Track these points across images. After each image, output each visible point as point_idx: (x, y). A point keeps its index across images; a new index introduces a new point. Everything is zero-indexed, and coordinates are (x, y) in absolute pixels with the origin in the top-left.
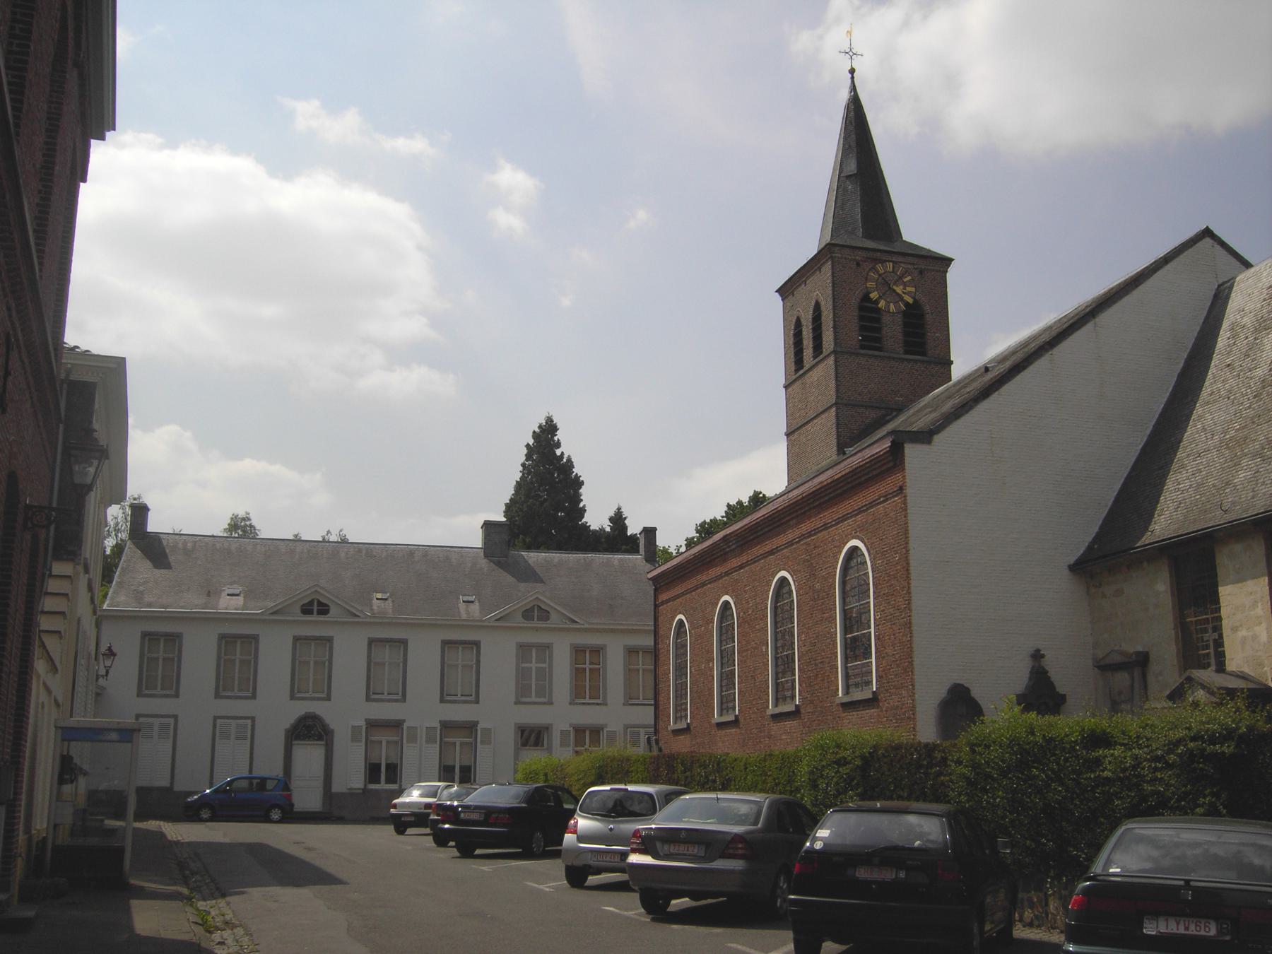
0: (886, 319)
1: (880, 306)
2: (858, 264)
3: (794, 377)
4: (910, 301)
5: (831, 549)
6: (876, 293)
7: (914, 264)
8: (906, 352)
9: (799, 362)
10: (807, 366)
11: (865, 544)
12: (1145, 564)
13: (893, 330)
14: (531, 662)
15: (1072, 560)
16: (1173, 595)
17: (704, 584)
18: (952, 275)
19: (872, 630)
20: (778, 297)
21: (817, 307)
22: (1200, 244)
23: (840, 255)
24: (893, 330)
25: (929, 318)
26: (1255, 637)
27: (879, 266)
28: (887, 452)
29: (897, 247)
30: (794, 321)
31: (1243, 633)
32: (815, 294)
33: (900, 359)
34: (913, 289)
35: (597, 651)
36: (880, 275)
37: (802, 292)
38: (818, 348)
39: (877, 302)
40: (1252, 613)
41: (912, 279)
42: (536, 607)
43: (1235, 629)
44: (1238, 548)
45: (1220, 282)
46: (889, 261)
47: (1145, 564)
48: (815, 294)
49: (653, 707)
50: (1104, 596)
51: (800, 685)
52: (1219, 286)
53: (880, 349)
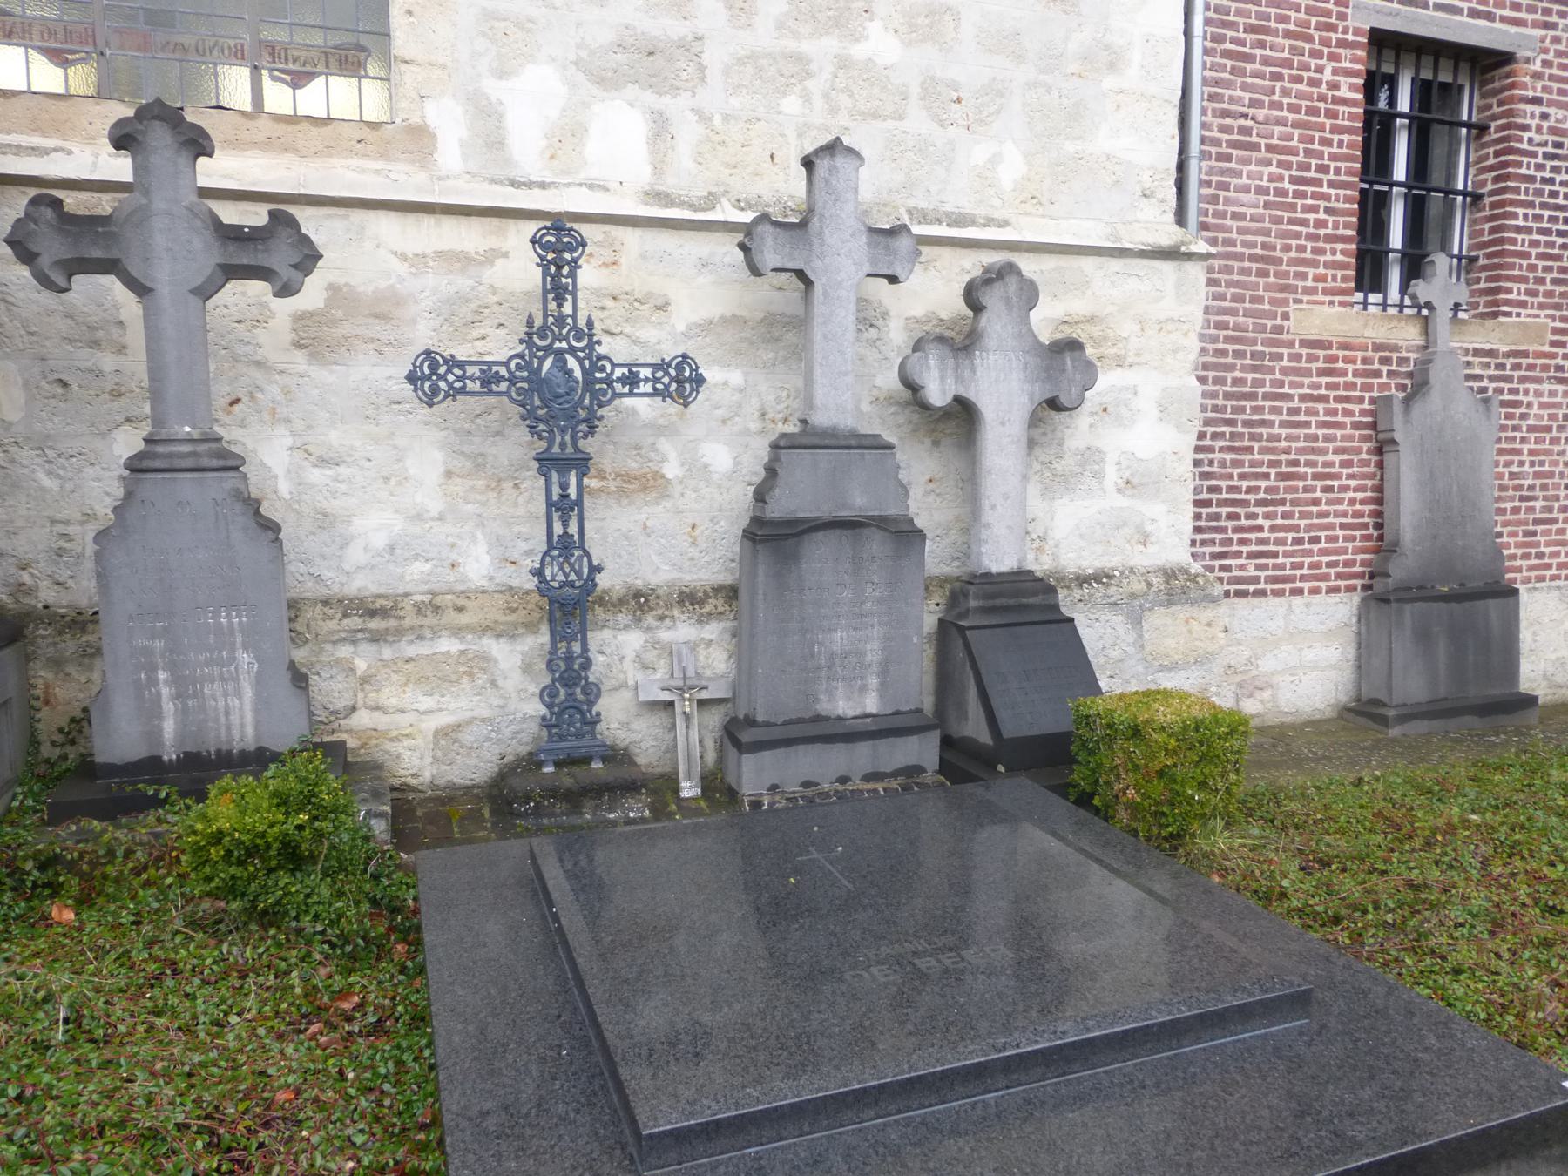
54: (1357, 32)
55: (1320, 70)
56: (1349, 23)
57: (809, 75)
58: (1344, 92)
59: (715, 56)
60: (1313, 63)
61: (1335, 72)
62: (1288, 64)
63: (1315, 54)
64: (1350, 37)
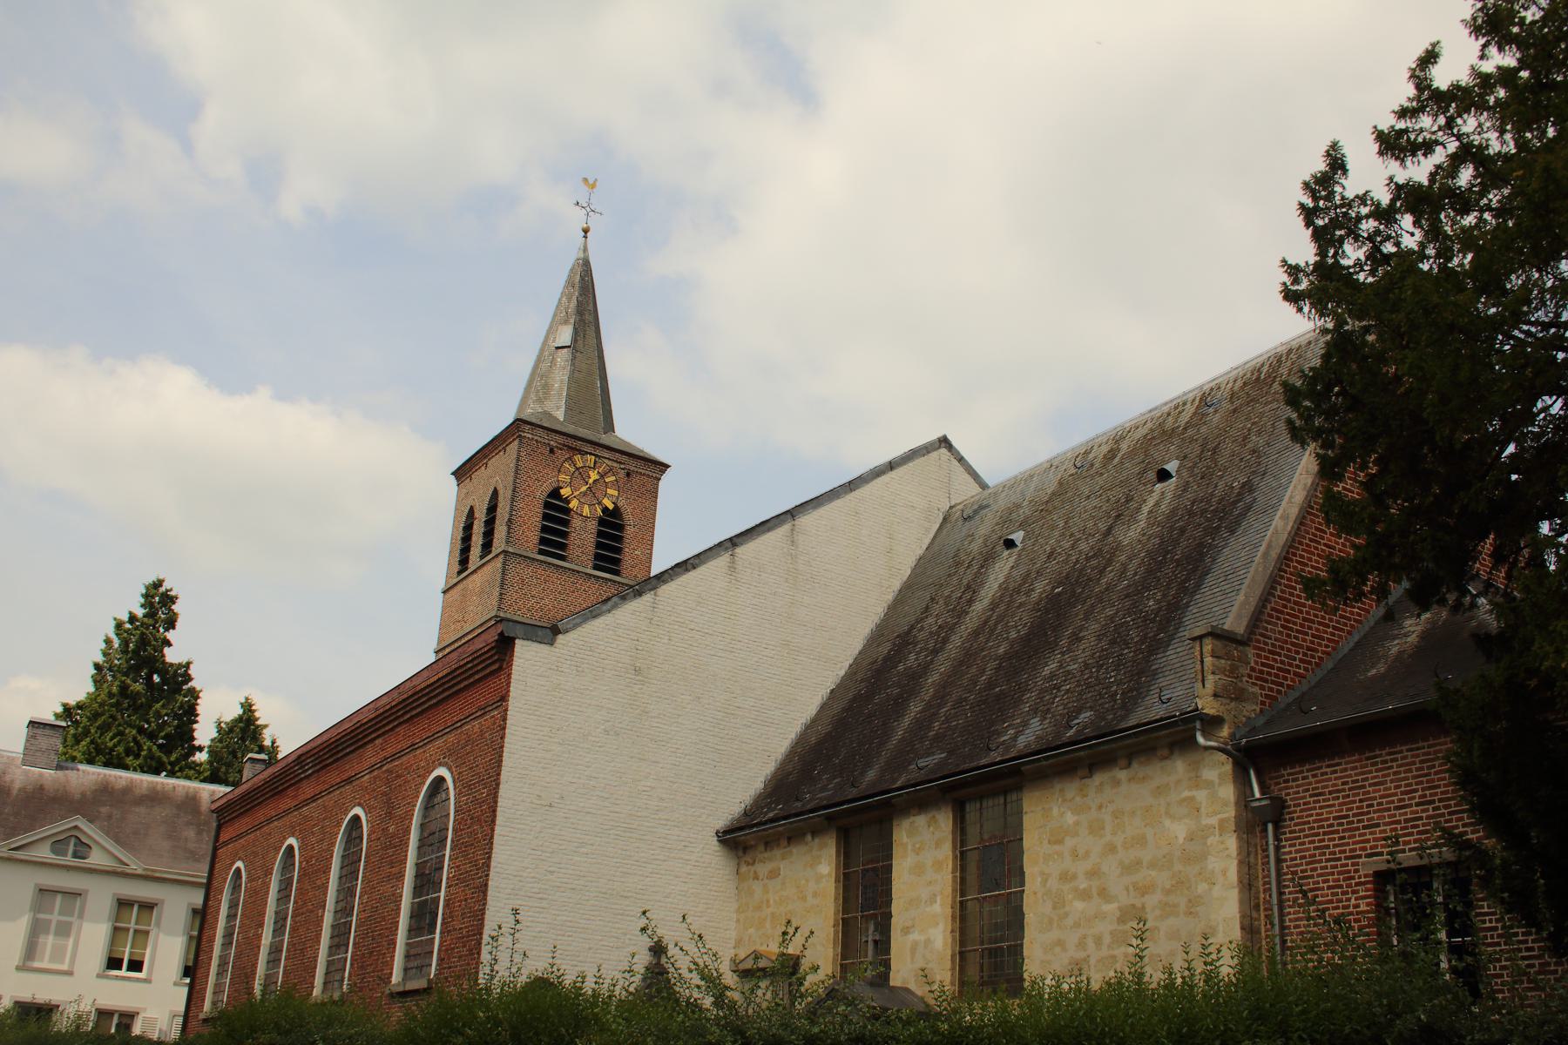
0: (576, 522)
1: (571, 506)
2: (552, 451)
3: (455, 581)
4: (611, 506)
5: (413, 779)
6: (569, 489)
7: (620, 463)
8: (596, 567)
9: (464, 562)
10: (472, 567)
11: (452, 774)
12: (809, 837)
13: (583, 536)
14: (60, 914)
15: (721, 823)
16: (837, 881)
17: (270, 821)
18: (666, 483)
19: (442, 894)
20: (453, 480)
21: (495, 493)
22: (934, 454)
23: (530, 436)
24: (583, 536)
25: (630, 531)
26: (928, 942)
27: (577, 458)
28: (492, 648)
29: (605, 439)
30: (467, 511)
31: (915, 936)
32: (495, 479)
33: (586, 574)
34: (616, 493)
35: (148, 907)
36: (577, 469)
37: (481, 475)
38: (487, 547)
39: (567, 501)
40: (928, 909)
41: (616, 480)
42: (73, 841)
43: (906, 931)
44: (920, 820)
45: (953, 504)
46: (591, 454)
47: (809, 837)
48: (495, 479)
49: (186, 990)
50: (756, 877)
51: (352, 965)
52: (951, 507)
53: (562, 558)
54: (1366, 876)
55: (1349, 900)
56: (1361, 873)
57: (1117, 961)
58: (1363, 908)
59: (1092, 961)
60: (1344, 897)
61: (1356, 899)
62: (1331, 902)
63: (1344, 893)
64: (1363, 880)
